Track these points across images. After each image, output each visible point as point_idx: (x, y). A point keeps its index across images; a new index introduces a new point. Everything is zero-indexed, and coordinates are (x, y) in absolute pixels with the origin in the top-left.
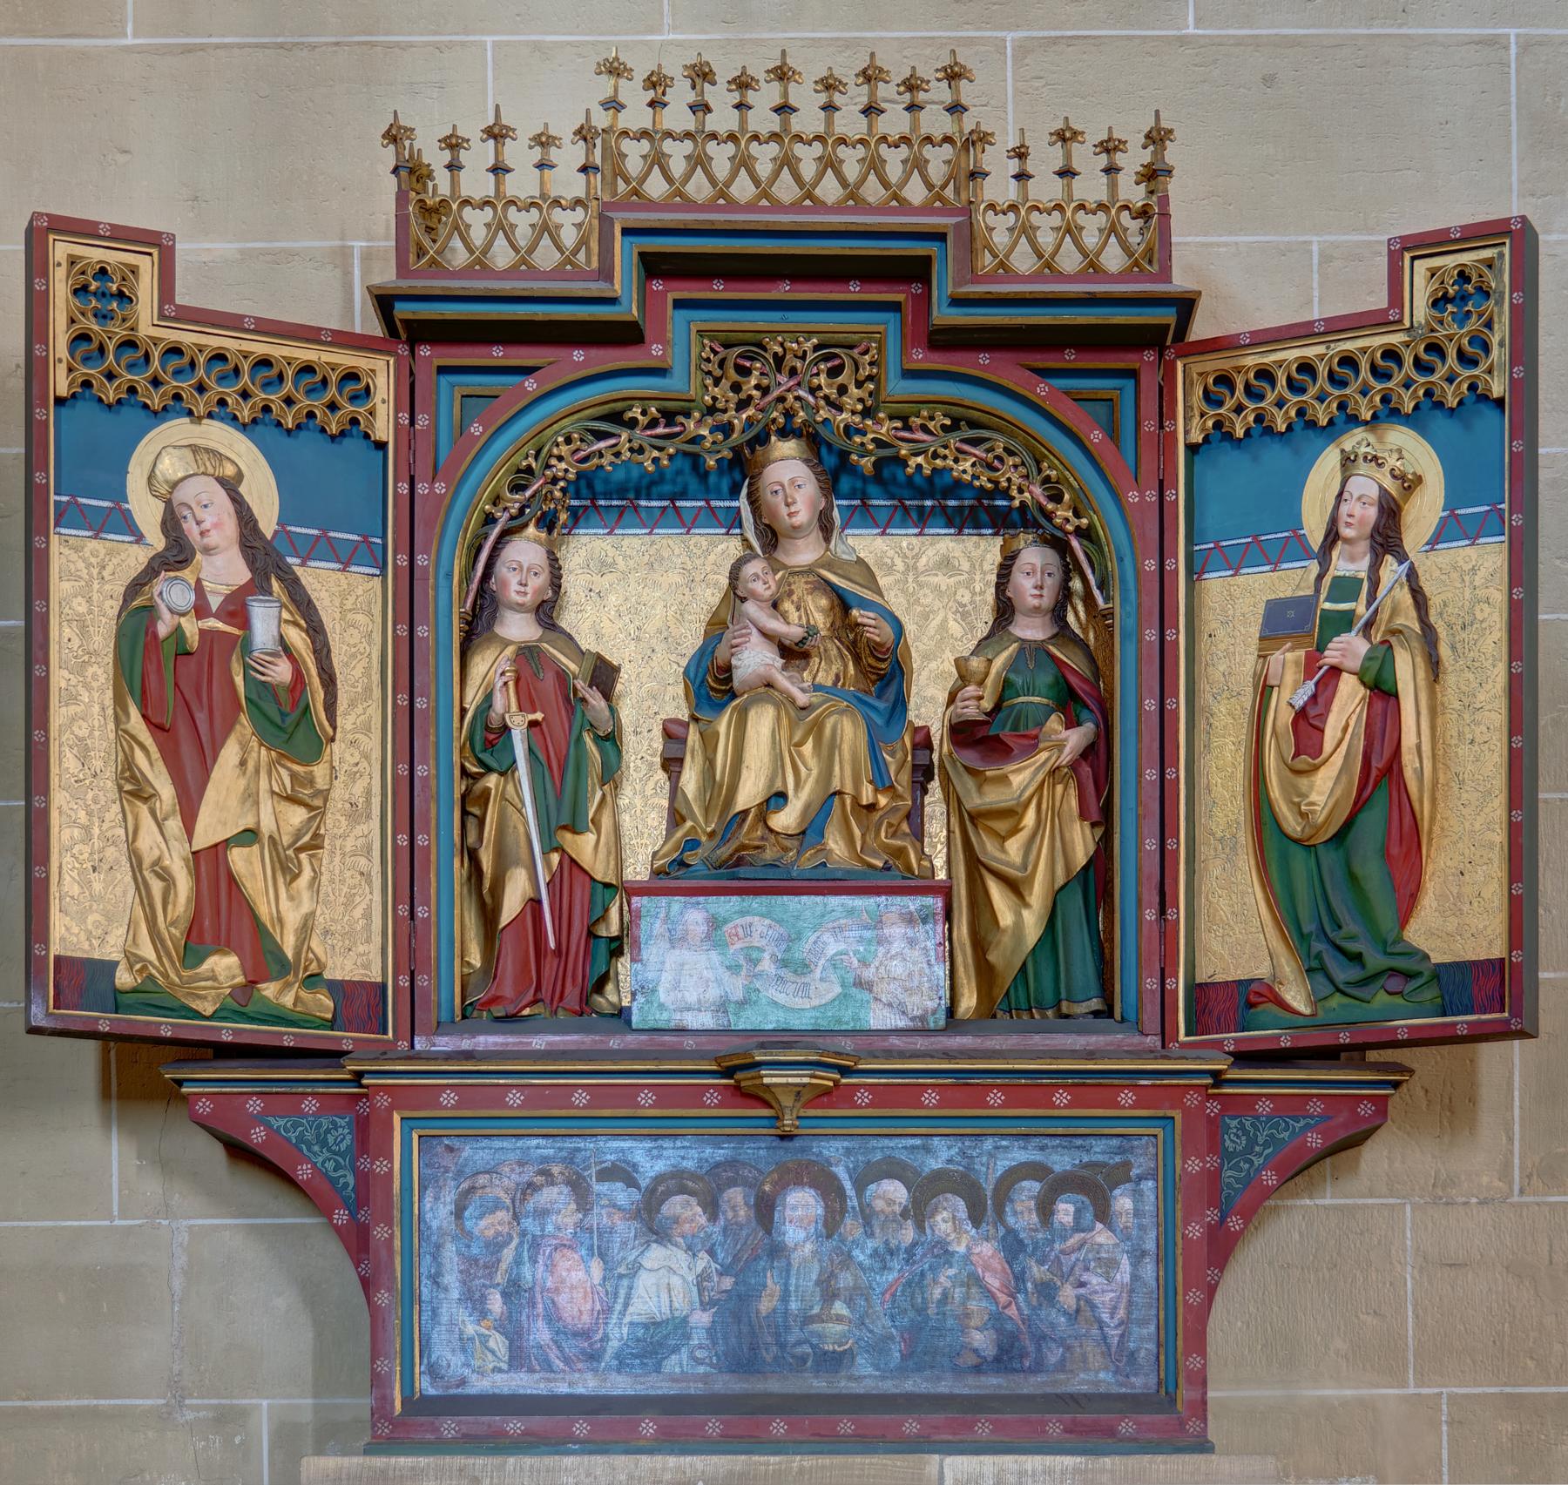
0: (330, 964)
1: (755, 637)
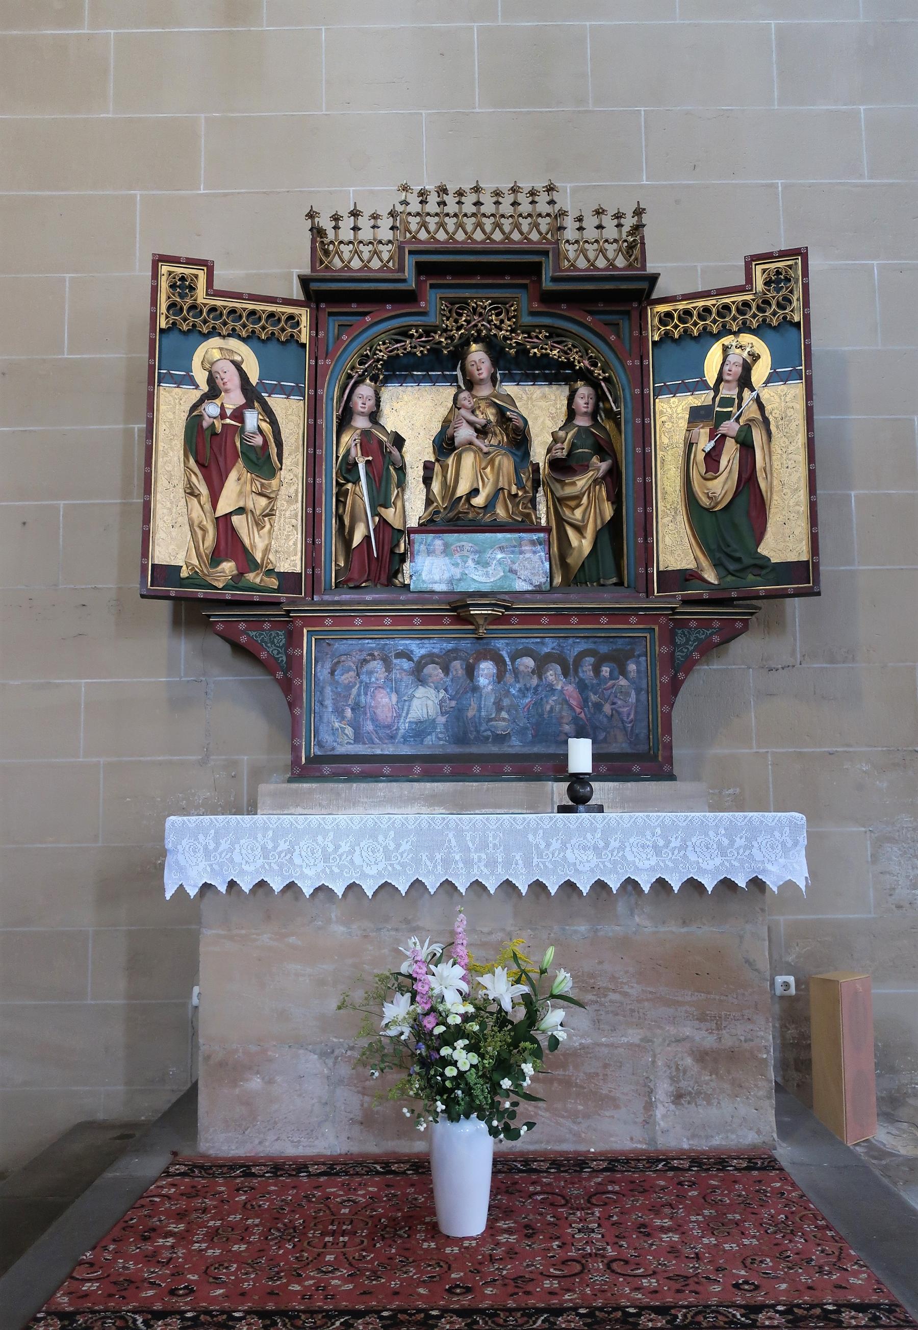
0: (278, 565)
1: (465, 424)
